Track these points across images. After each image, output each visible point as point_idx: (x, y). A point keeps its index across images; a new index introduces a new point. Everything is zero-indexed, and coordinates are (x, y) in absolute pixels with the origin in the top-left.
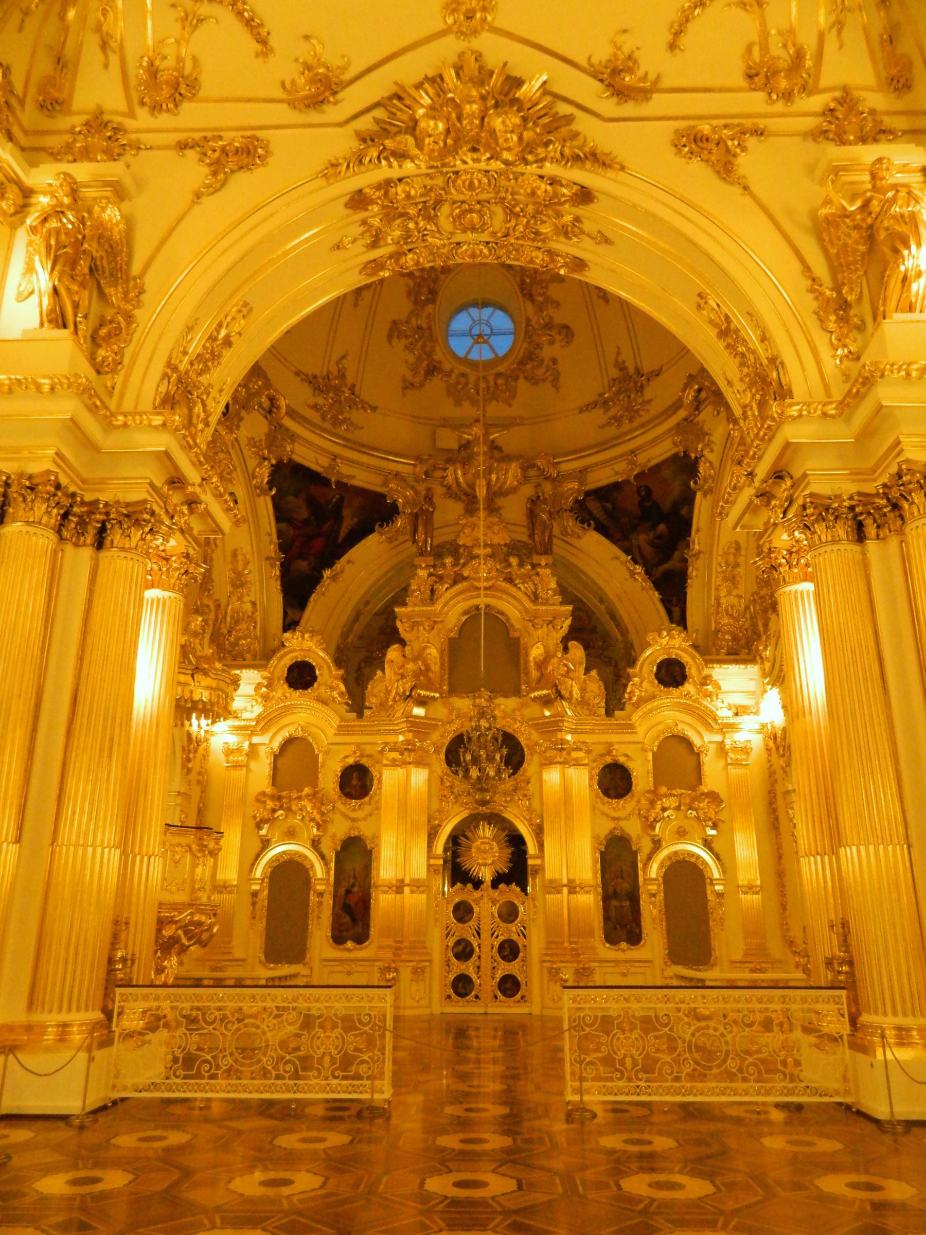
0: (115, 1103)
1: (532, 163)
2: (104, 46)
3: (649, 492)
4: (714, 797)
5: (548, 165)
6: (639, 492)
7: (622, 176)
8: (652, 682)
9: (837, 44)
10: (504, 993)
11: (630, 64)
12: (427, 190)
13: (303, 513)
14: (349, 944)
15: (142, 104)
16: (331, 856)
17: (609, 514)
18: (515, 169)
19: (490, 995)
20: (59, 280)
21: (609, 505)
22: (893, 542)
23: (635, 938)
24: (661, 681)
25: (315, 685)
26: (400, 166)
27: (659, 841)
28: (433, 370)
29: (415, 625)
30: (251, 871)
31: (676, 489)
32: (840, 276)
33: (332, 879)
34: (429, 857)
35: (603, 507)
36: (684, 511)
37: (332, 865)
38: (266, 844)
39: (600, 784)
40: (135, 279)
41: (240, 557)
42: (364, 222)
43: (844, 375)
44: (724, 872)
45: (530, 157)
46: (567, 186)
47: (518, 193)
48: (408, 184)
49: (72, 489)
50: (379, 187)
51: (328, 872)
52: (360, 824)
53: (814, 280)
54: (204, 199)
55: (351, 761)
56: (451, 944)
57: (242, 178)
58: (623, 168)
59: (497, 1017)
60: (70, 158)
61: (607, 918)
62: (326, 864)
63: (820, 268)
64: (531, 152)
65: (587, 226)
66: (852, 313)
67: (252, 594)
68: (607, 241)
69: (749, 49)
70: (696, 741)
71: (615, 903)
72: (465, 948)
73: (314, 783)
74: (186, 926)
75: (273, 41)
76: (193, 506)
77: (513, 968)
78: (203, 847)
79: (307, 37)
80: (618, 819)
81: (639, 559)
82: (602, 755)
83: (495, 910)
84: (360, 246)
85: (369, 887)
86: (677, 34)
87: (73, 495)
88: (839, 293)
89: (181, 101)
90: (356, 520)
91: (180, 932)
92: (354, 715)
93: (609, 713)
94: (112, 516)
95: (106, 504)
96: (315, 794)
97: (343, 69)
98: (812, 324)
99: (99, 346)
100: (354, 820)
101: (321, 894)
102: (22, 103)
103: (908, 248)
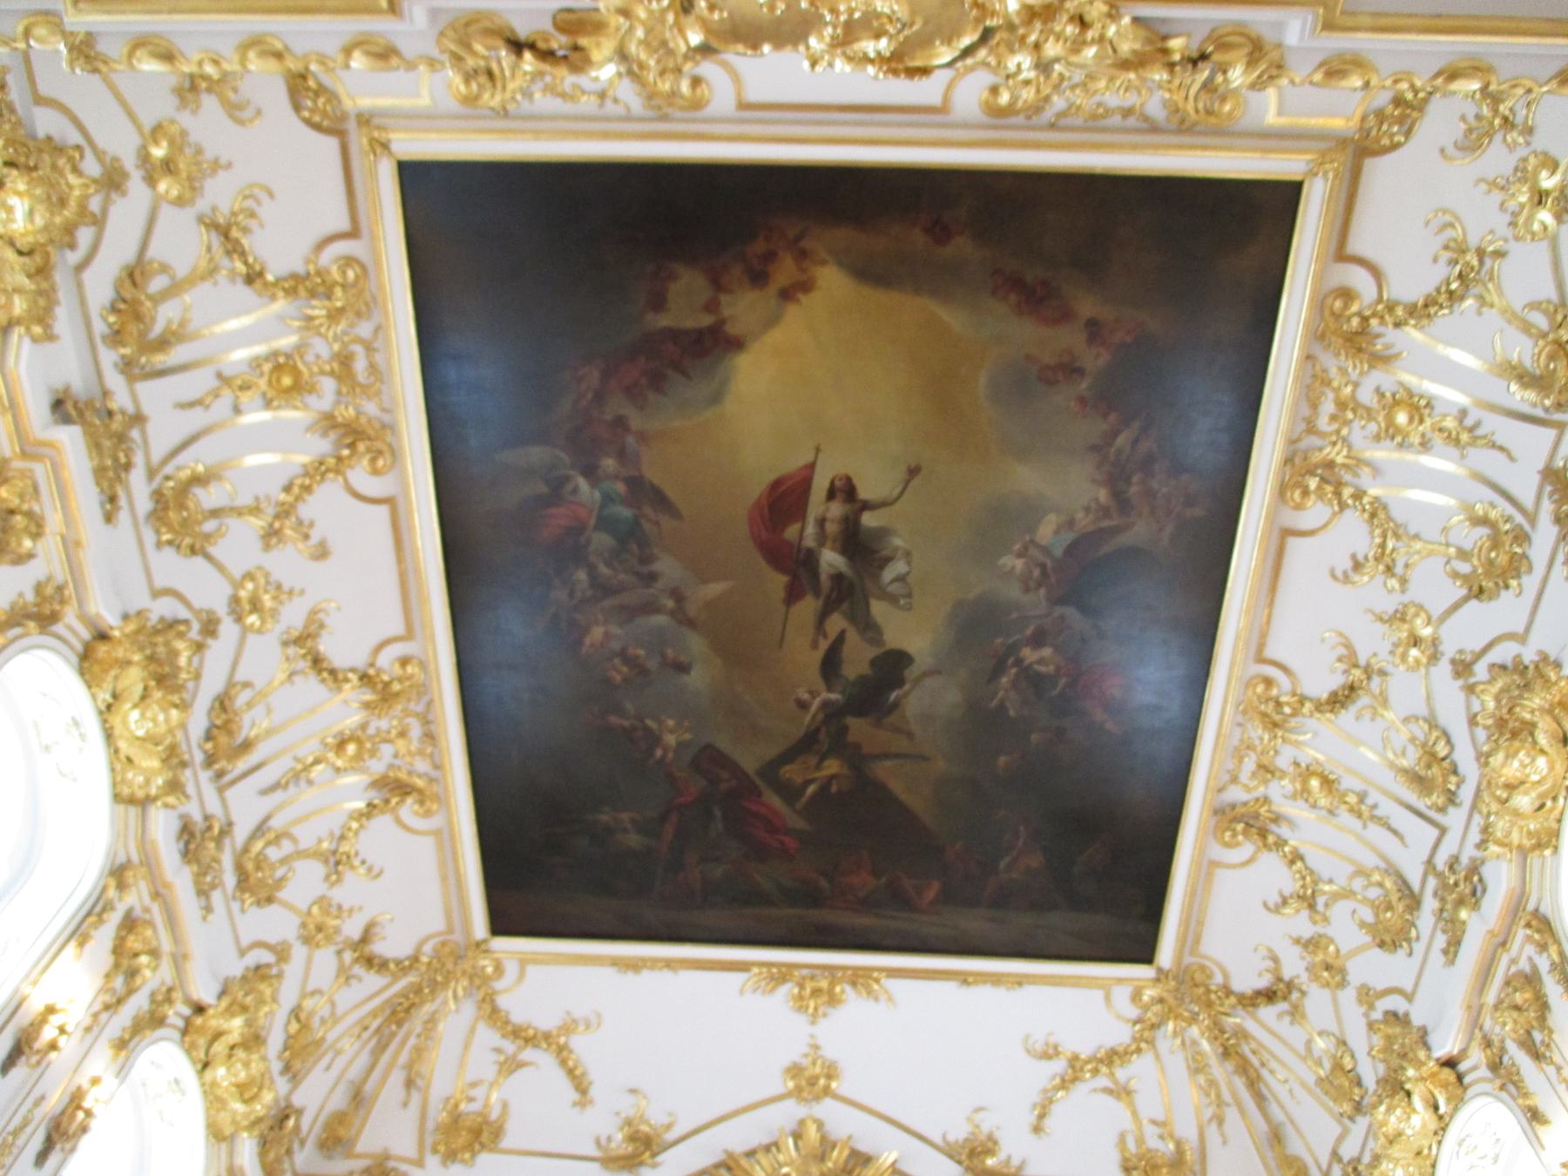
2: (409, 1083)
9: (1220, 1140)
11: (990, 1144)
15: (435, 1151)
69: (1122, 1139)
75: (594, 1092)
79: (633, 1091)
86: (1042, 1116)
89: (479, 1152)
97: (669, 1127)
102: (303, 1143)
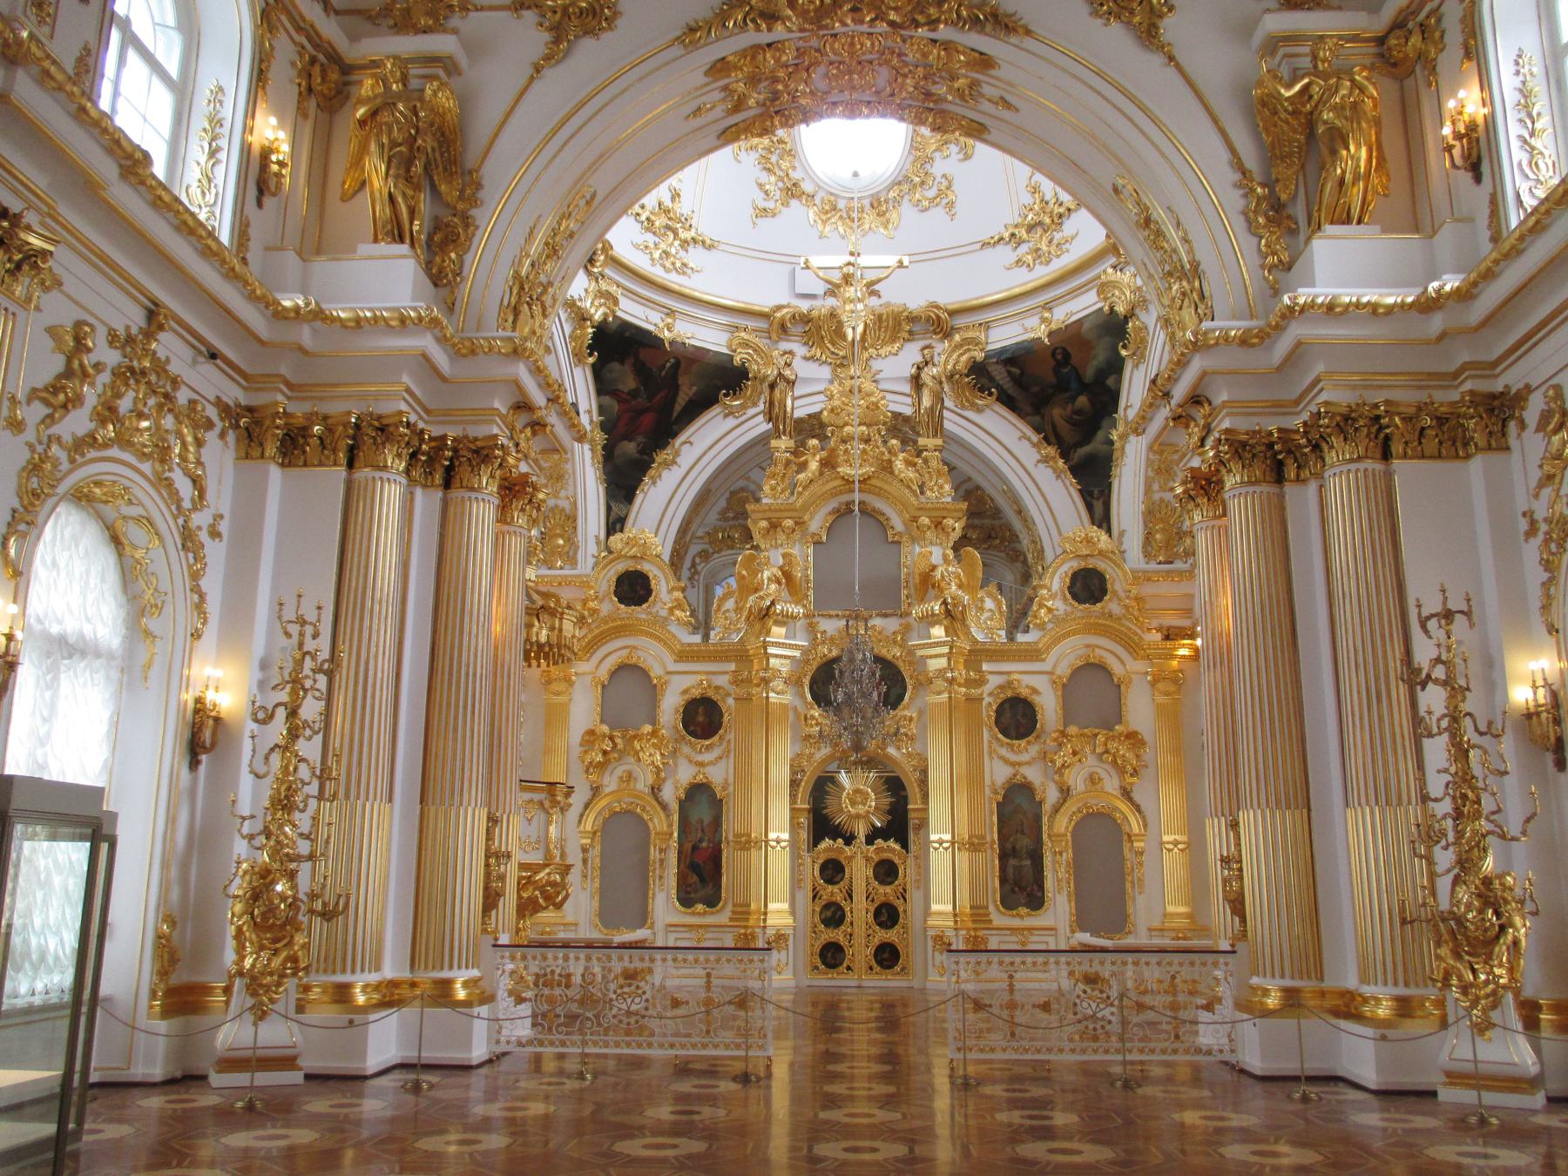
0: (498, 1057)
1: (922, 25)
3: (1067, 355)
4: (1133, 738)
5: (942, 26)
6: (1053, 354)
7: (1029, 43)
8: (1065, 599)
10: (880, 963)
12: (800, 53)
13: (629, 382)
14: (700, 907)
16: (674, 806)
17: (1017, 381)
18: (902, 32)
19: (864, 967)
20: (395, 186)
21: (1016, 371)
22: (1312, 487)
23: (1036, 901)
24: (1075, 596)
25: (651, 599)
26: (769, 30)
27: (1068, 790)
28: (793, 191)
29: (774, 526)
30: (580, 822)
31: (1100, 357)
32: (1274, 171)
33: (676, 835)
34: (792, 810)
35: (1009, 372)
36: (1110, 382)
37: (676, 818)
39: (997, 723)
40: (470, 172)
42: (725, 88)
43: (1272, 288)
44: (1145, 826)
45: (921, 18)
46: (964, 53)
47: (906, 55)
48: (779, 50)
49: (421, 425)
50: (743, 54)
51: (670, 825)
52: (708, 770)
53: (1244, 173)
54: (545, 72)
55: (696, 693)
56: (818, 909)
57: (588, 43)
58: (1028, 32)
59: (872, 991)
60: (391, 22)
61: (1003, 881)
63: (1251, 161)
64: (922, 12)
65: (986, 90)
66: (1284, 214)
67: (571, 488)
68: (1008, 105)
70: (1117, 669)
71: (1012, 862)
72: (834, 913)
73: (653, 721)
74: (543, 886)
76: (537, 428)
77: (891, 936)
78: (555, 803)
80: (1020, 764)
81: (1052, 439)
82: (1001, 687)
83: (870, 873)
84: (719, 111)
85: (720, 843)
87: (422, 432)
88: (1272, 191)
90: (695, 389)
91: (537, 893)
92: (697, 639)
93: (1011, 638)
94: (461, 453)
95: (455, 440)
96: (654, 733)
98: (1240, 223)
99: (436, 254)
100: (701, 764)
103: (1348, 149)
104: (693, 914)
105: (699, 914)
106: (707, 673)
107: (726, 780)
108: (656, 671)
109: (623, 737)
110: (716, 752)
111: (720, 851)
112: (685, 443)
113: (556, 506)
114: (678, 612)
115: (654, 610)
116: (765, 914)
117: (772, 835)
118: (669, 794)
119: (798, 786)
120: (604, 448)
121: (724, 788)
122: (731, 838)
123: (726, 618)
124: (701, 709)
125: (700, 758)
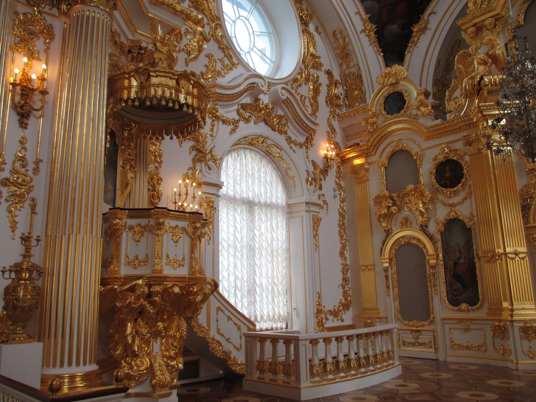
14: (464, 306)
16: (438, 237)
25: (405, 106)
29: (479, 29)
30: (381, 253)
34: (526, 228)
37: (439, 244)
38: (388, 233)
41: (339, 36)
51: (436, 250)
52: (457, 208)
55: (441, 158)
62: (434, 244)
73: (417, 181)
85: (473, 259)
92: (439, 121)
96: (415, 190)
100: (452, 205)
101: (433, 267)
104: (460, 310)
105: (464, 311)
106: (448, 143)
107: (472, 214)
108: (414, 149)
109: (398, 197)
110: (462, 195)
111: (474, 264)
112: (430, 14)
113: (350, 72)
114: (423, 109)
115: (409, 113)
116: (512, 310)
117: (508, 250)
118: (432, 228)
119: (529, 209)
120: (376, 33)
121: (471, 219)
122: (480, 254)
123: (456, 103)
124: (447, 168)
125: (451, 201)
